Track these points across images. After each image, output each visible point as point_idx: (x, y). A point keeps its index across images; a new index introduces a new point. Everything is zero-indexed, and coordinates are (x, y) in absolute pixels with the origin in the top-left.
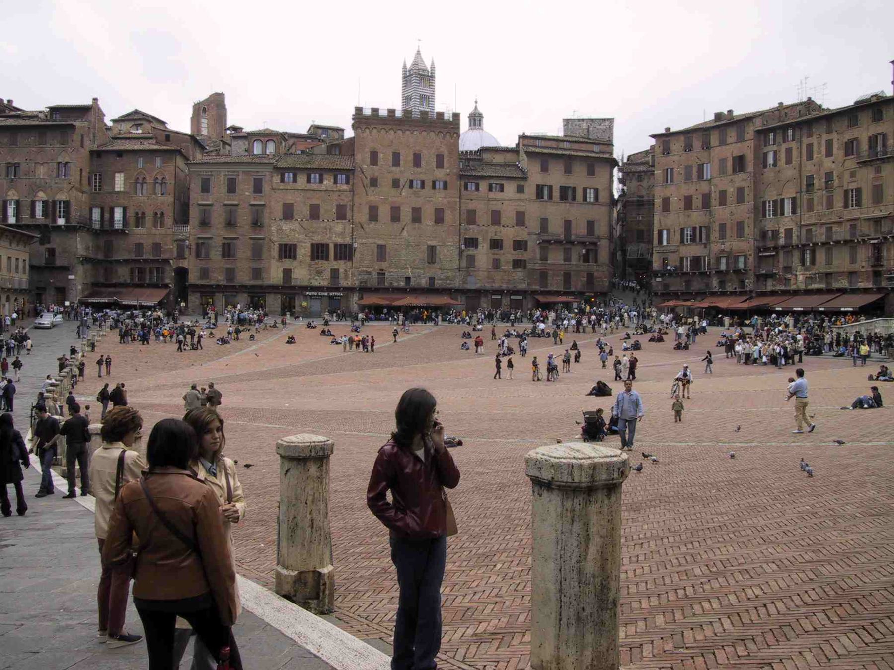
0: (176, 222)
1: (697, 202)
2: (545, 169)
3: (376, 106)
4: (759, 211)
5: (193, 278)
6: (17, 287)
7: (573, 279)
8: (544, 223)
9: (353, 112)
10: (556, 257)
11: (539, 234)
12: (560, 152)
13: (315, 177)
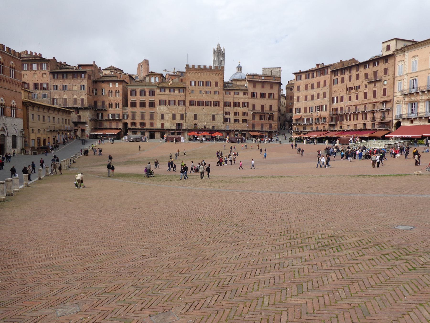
0: (123, 106)
1: (309, 98)
2: (254, 86)
3: (193, 64)
4: (332, 100)
5: (129, 126)
6: (66, 129)
7: (264, 126)
8: (254, 106)
9: (185, 66)
12: (261, 80)
13: (172, 90)
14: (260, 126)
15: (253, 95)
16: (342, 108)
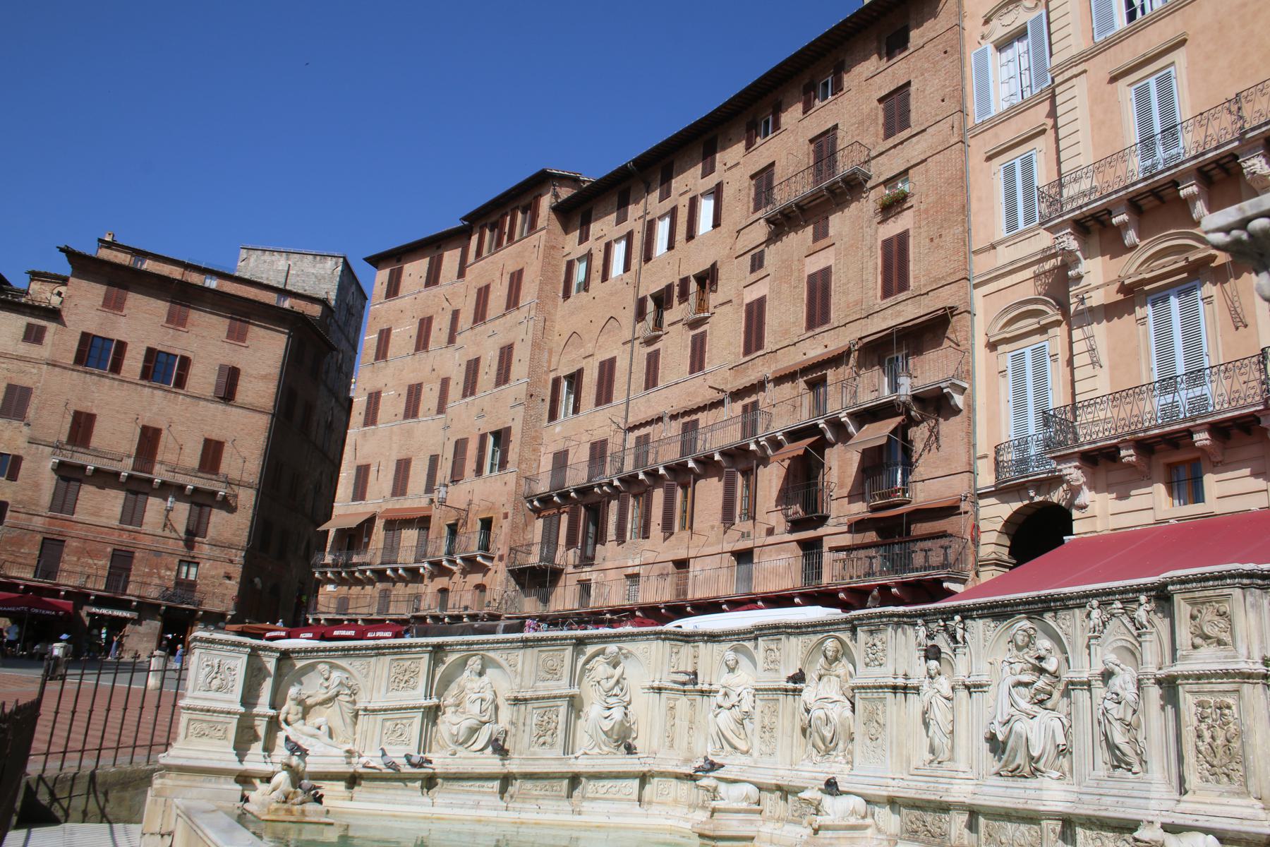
7: (138, 570)
8: (82, 426)
10: (101, 508)
11: (58, 447)
14: (105, 563)
15: (97, 354)
16: (604, 443)
